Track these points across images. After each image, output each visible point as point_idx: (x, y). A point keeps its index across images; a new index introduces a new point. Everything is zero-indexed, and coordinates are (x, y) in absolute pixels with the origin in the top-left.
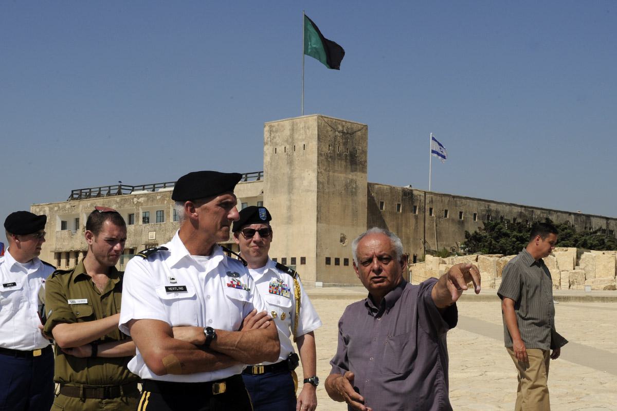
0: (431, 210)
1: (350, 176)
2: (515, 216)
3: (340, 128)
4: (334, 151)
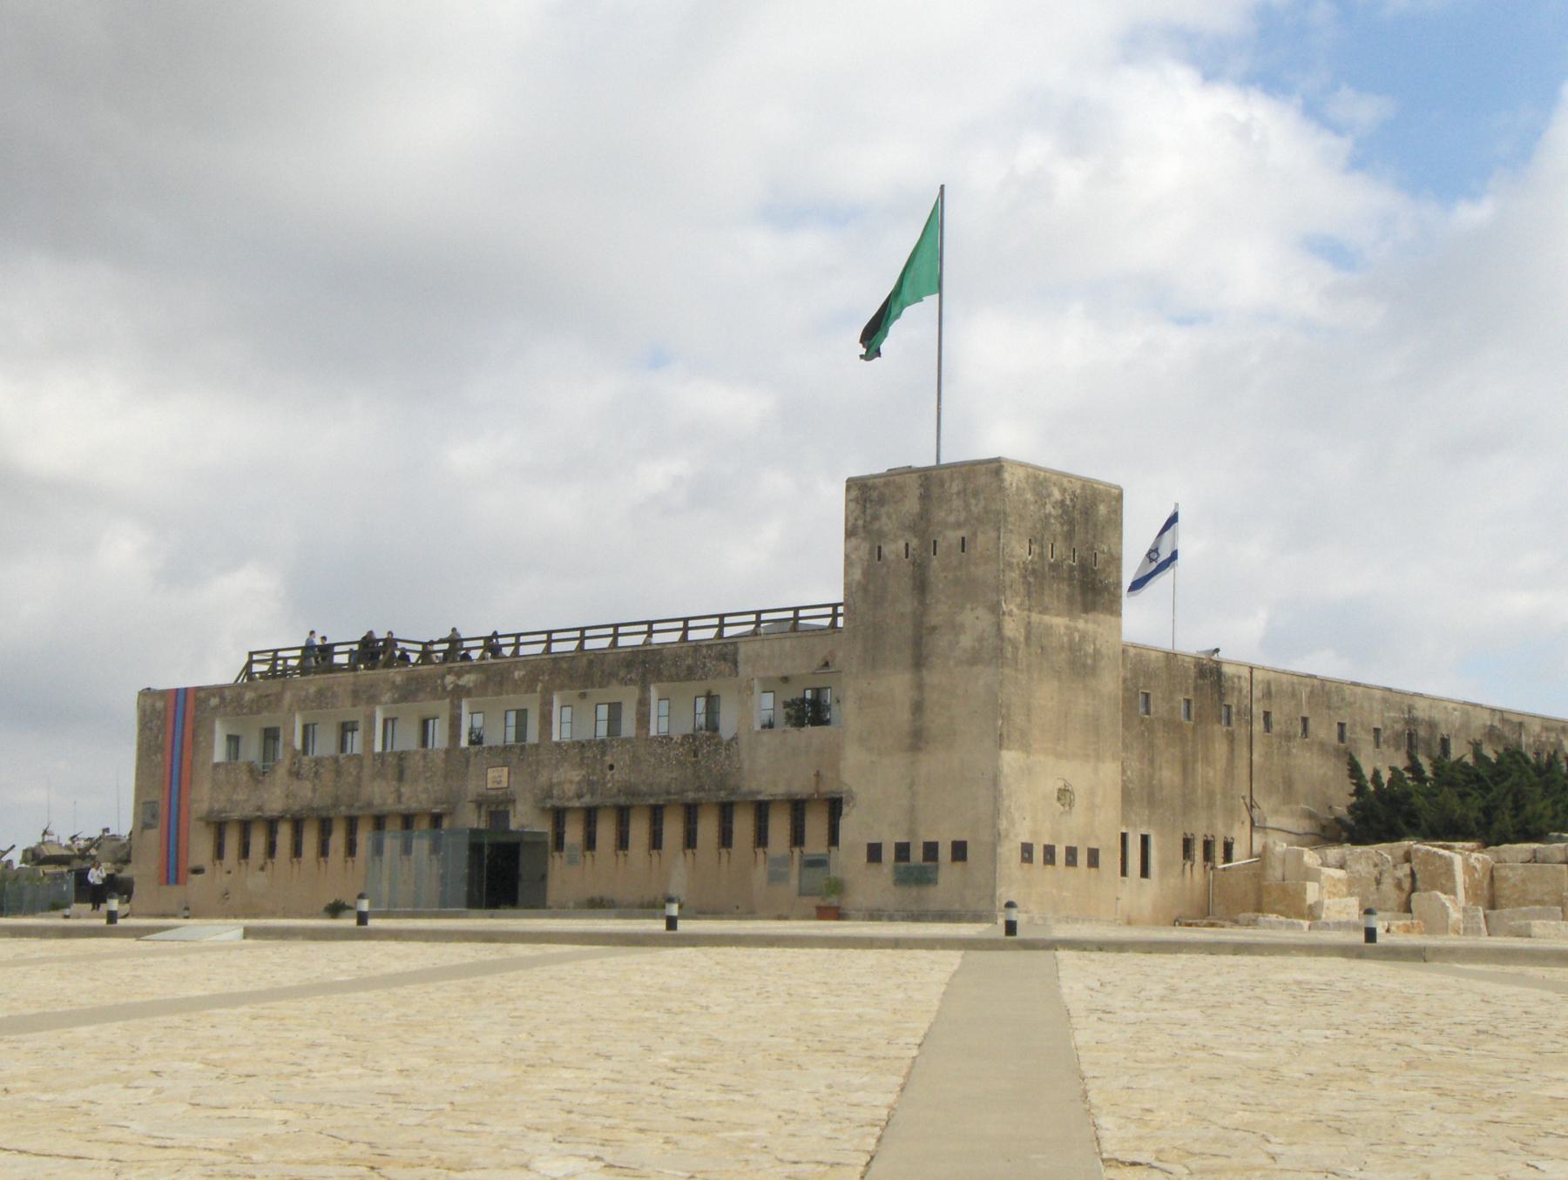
0: (1267, 715)
1: (1081, 624)
2: (1478, 738)
3: (1057, 495)
4: (1041, 555)
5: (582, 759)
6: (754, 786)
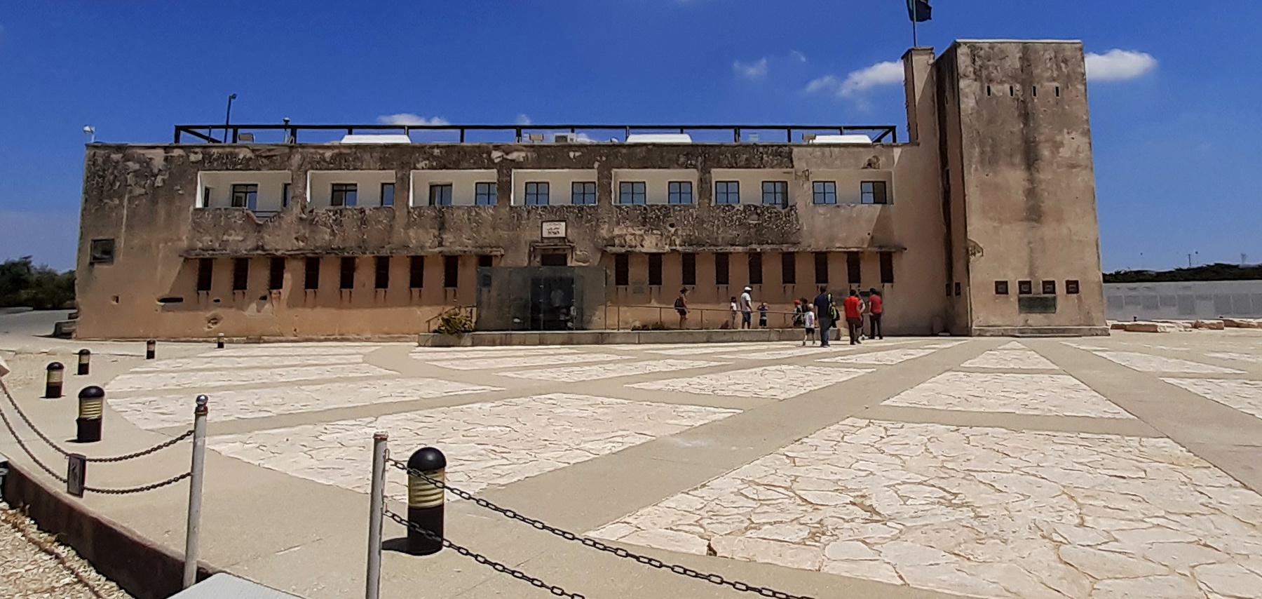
5: (644, 219)
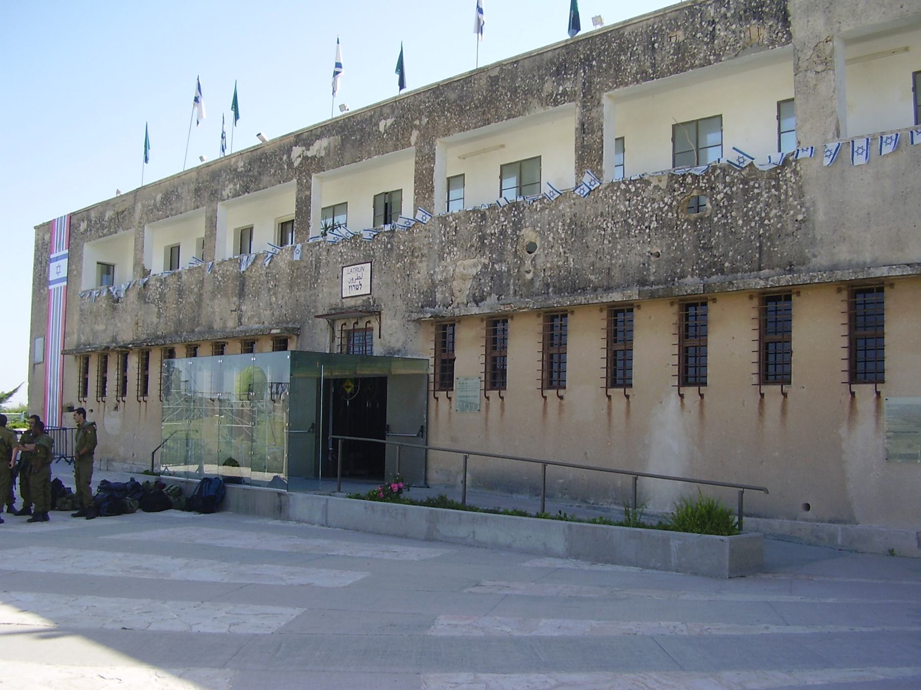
5: (482, 238)
6: (843, 254)
